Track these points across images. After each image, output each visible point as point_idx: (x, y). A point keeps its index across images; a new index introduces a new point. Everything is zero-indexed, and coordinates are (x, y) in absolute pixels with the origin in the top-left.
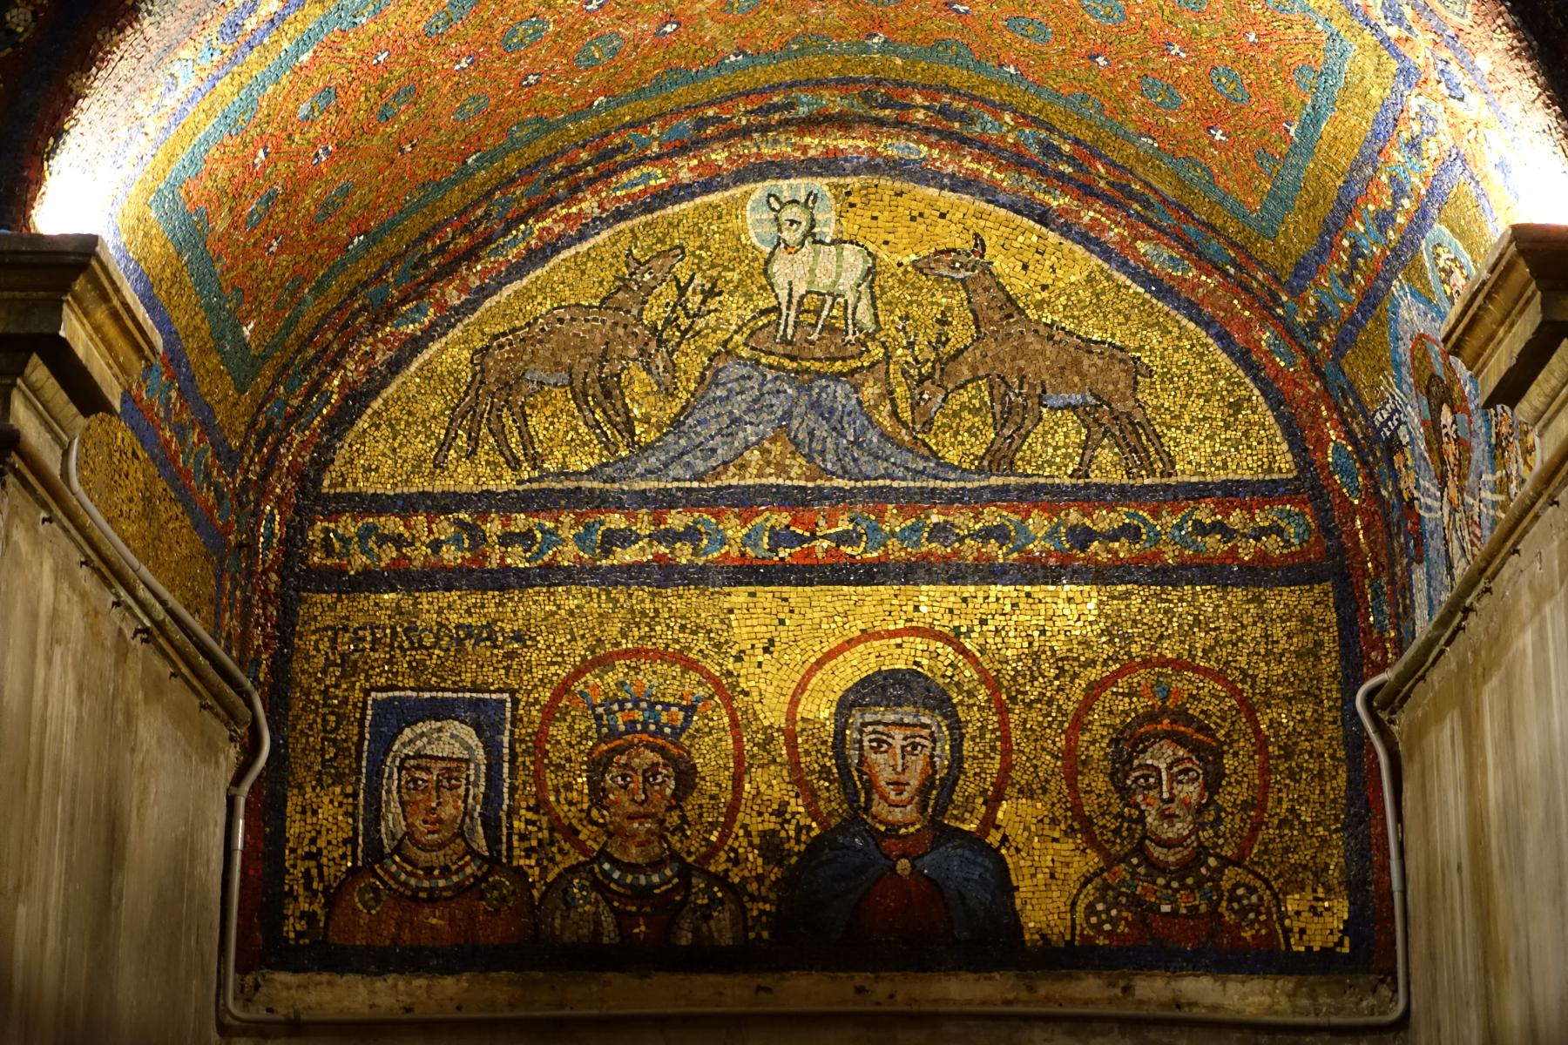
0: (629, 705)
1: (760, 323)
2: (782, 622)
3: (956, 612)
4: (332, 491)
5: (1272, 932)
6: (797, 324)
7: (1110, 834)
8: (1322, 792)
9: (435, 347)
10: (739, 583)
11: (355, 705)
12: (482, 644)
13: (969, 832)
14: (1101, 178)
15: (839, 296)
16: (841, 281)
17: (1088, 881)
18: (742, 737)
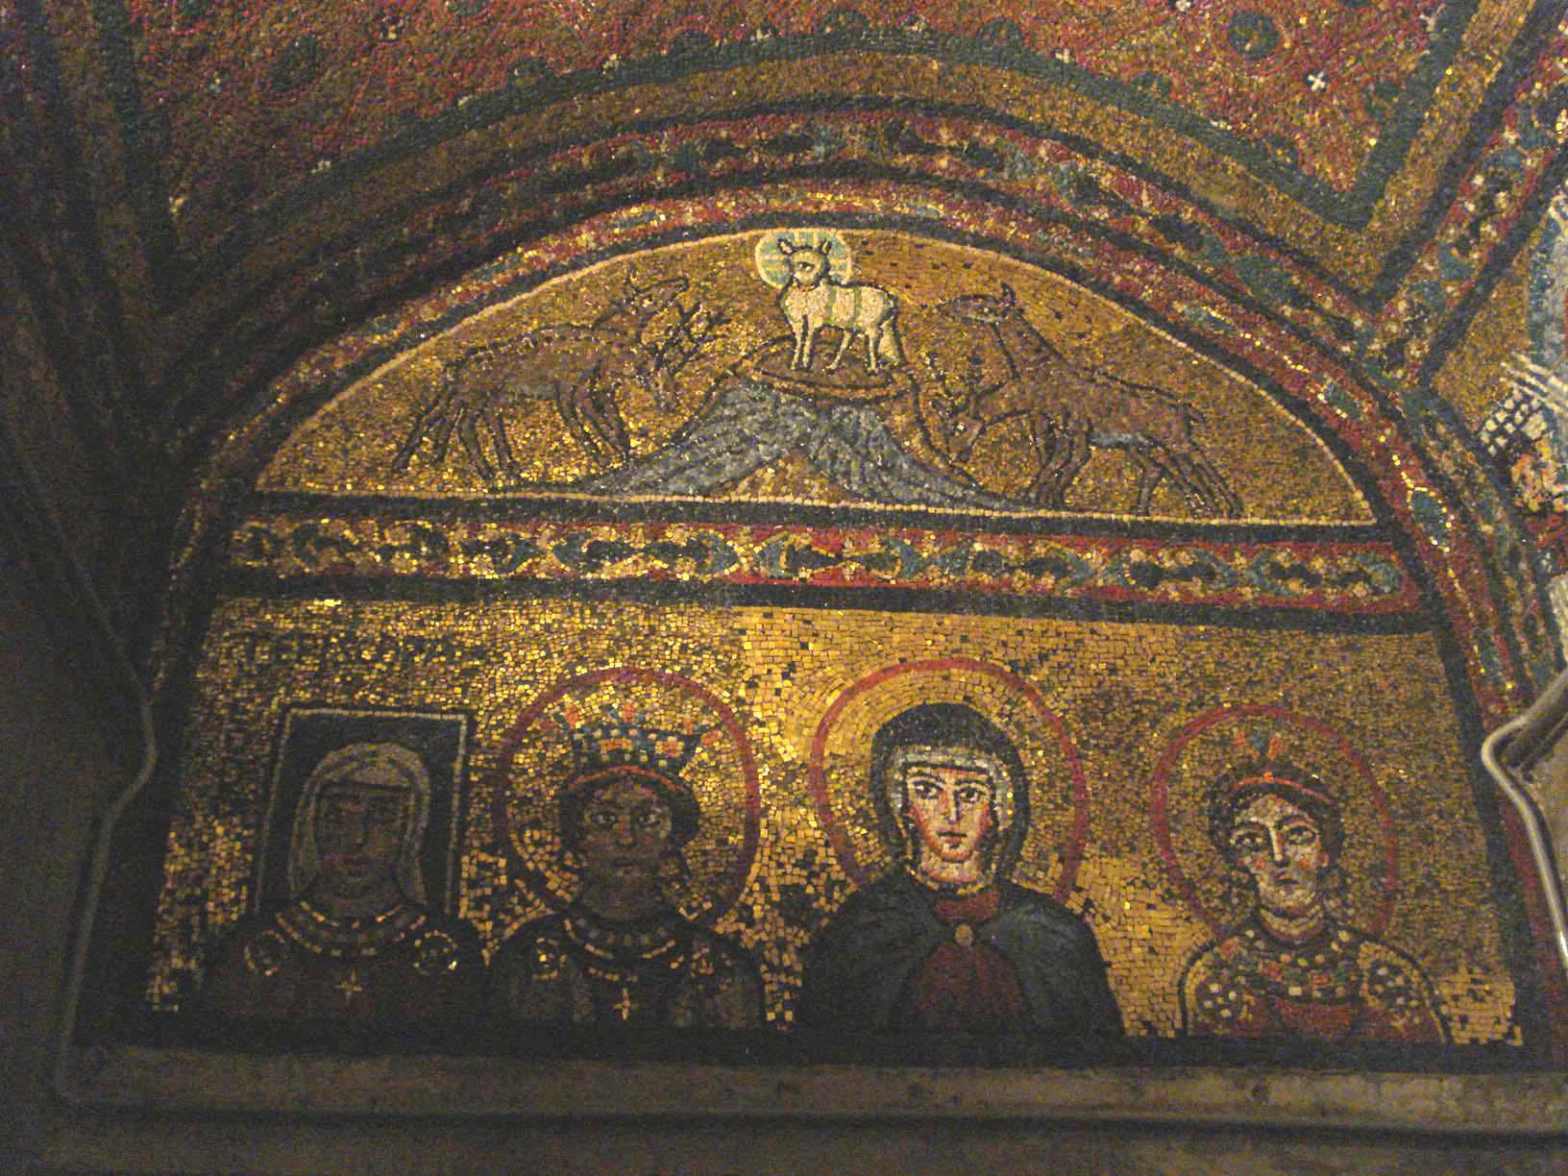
0: (615, 732)
1: (773, 350)
2: (804, 646)
3: (1011, 645)
4: (267, 491)
5: (1427, 1023)
6: (812, 355)
7: (1216, 902)
8: (1461, 856)
9: (402, 358)
10: (749, 604)
11: (269, 721)
12: (435, 660)
13: (1044, 896)
14: (1144, 215)
15: (859, 331)
16: (860, 318)
17: (1197, 956)
18: (757, 774)
